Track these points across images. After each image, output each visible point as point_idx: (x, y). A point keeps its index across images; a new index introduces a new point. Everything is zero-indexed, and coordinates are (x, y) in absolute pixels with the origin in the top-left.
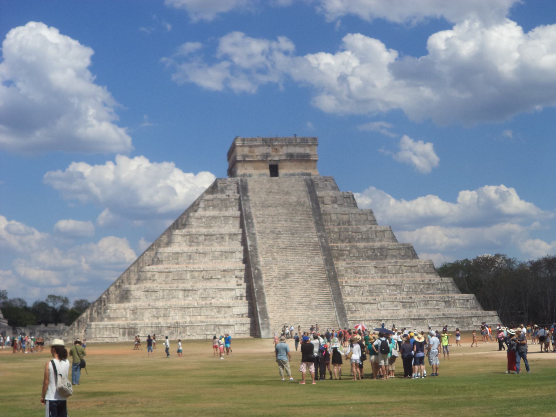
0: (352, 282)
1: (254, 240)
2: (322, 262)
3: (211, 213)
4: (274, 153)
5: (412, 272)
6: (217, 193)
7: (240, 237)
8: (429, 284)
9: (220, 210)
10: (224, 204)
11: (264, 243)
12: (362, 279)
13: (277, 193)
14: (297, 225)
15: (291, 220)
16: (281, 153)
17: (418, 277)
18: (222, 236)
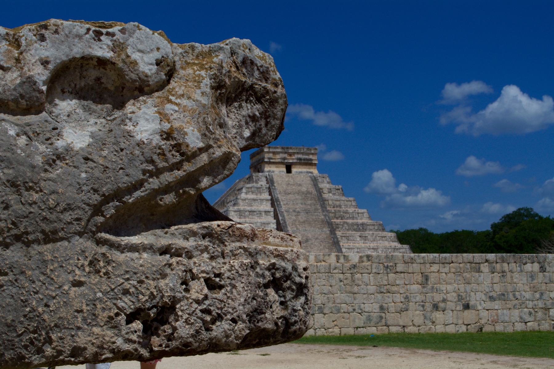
0: (346, 245)
1: (283, 216)
2: (328, 232)
3: (251, 196)
4: (289, 158)
5: (383, 240)
6: (253, 183)
7: (272, 213)
8: (395, 249)
9: (257, 195)
10: (259, 190)
11: (290, 218)
12: (351, 244)
13: (294, 185)
14: (309, 207)
15: (305, 204)
16: (294, 157)
17: (387, 244)
18: (260, 213)
